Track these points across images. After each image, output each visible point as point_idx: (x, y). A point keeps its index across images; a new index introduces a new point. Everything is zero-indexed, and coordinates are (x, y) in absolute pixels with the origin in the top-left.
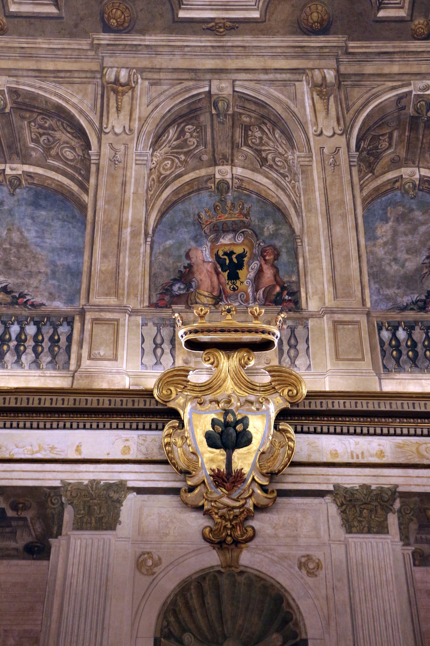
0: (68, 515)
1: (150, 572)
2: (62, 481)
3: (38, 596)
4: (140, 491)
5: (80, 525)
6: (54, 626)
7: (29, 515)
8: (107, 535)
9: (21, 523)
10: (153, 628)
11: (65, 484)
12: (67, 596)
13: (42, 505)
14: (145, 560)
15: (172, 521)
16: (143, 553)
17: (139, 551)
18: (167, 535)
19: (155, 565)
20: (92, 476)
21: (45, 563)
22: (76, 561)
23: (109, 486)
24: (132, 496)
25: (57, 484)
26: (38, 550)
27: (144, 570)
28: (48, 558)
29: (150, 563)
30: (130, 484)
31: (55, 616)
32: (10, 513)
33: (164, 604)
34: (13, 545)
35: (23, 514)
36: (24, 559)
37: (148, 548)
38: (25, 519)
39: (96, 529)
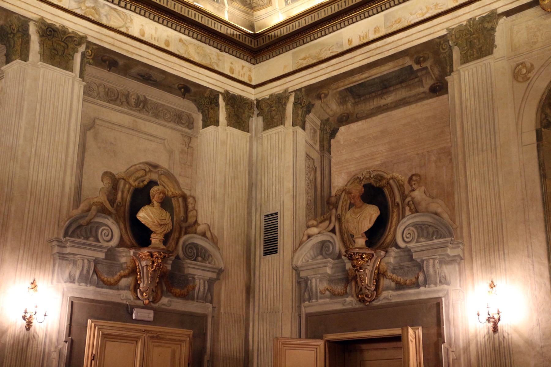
0: (456, 54)
1: (526, 79)
2: (447, 29)
3: (445, 122)
4: (508, 14)
5: (466, 59)
6: (459, 140)
7: (428, 64)
8: (487, 60)
9: (424, 72)
10: (534, 122)
11: (450, 30)
12: (465, 117)
13: (436, 53)
14: (520, 70)
15: (539, 30)
16: (518, 65)
17: (514, 64)
18: (535, 43)
19: (529, 71)
20: (468, 17)
21: (445, 96)
22: (467, 87)
23: (483, 19)
24: (503, 20)
25: (444, 32)
26: (439, 89)
27: (520, 79)
28: (447, 92)
29: (524, 71)
30: (500, 11)
31: (459, 133)
32: (416, 67)
33: (540, 101)
34: (421, 90)
35: (425, 65)
36: (431, 98)
37: (521, 59)
38: (426, 68)
39: (478, 58)
